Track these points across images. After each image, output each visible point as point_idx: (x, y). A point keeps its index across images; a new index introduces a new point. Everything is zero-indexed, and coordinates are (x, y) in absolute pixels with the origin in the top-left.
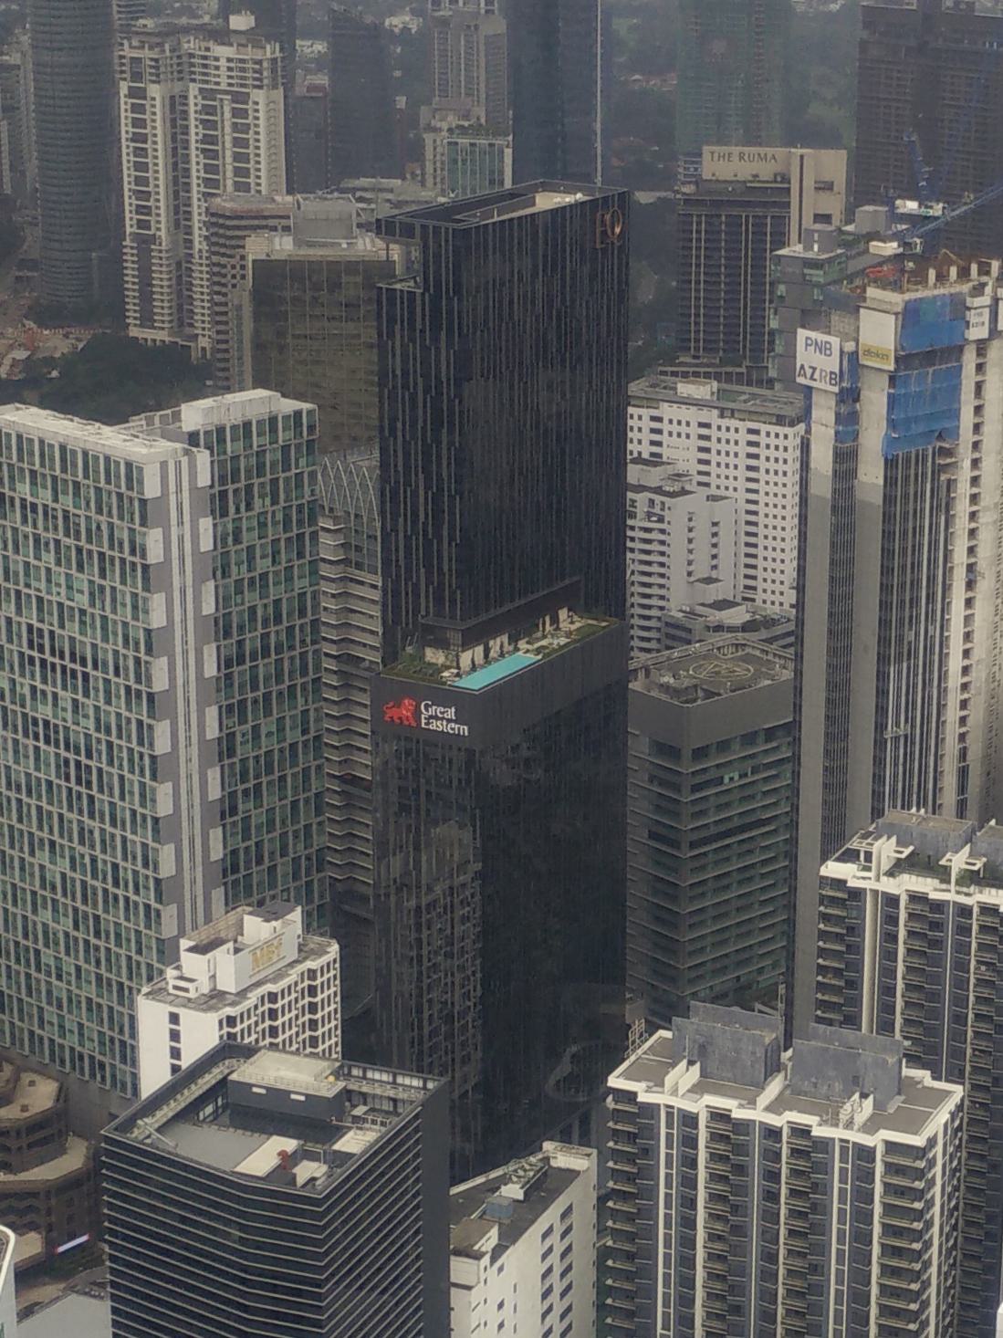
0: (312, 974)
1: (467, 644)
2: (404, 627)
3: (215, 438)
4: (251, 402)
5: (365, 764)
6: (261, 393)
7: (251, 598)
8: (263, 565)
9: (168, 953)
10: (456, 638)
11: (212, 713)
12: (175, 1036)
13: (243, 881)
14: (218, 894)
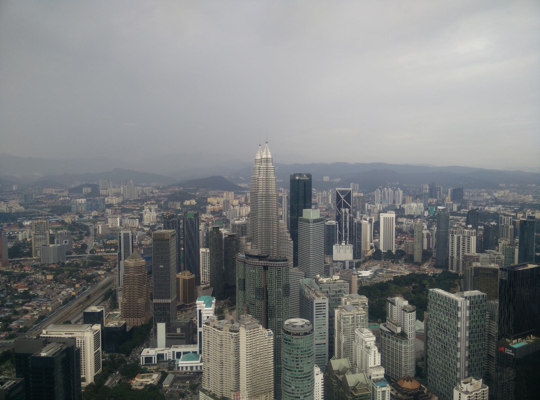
0: (484, 391)
1: (514, 339)
2: (502, 335)
3: (470, 298)
4: (476, 292)
5: (494, 354)
6: (477, 291)
7: (474, 324)
8: (476, 319)
9: (459, 380)
10: (512, 338)
11: (467, 342)
12: (460, 397)
13: (472, 371)
14: (467, 372)
